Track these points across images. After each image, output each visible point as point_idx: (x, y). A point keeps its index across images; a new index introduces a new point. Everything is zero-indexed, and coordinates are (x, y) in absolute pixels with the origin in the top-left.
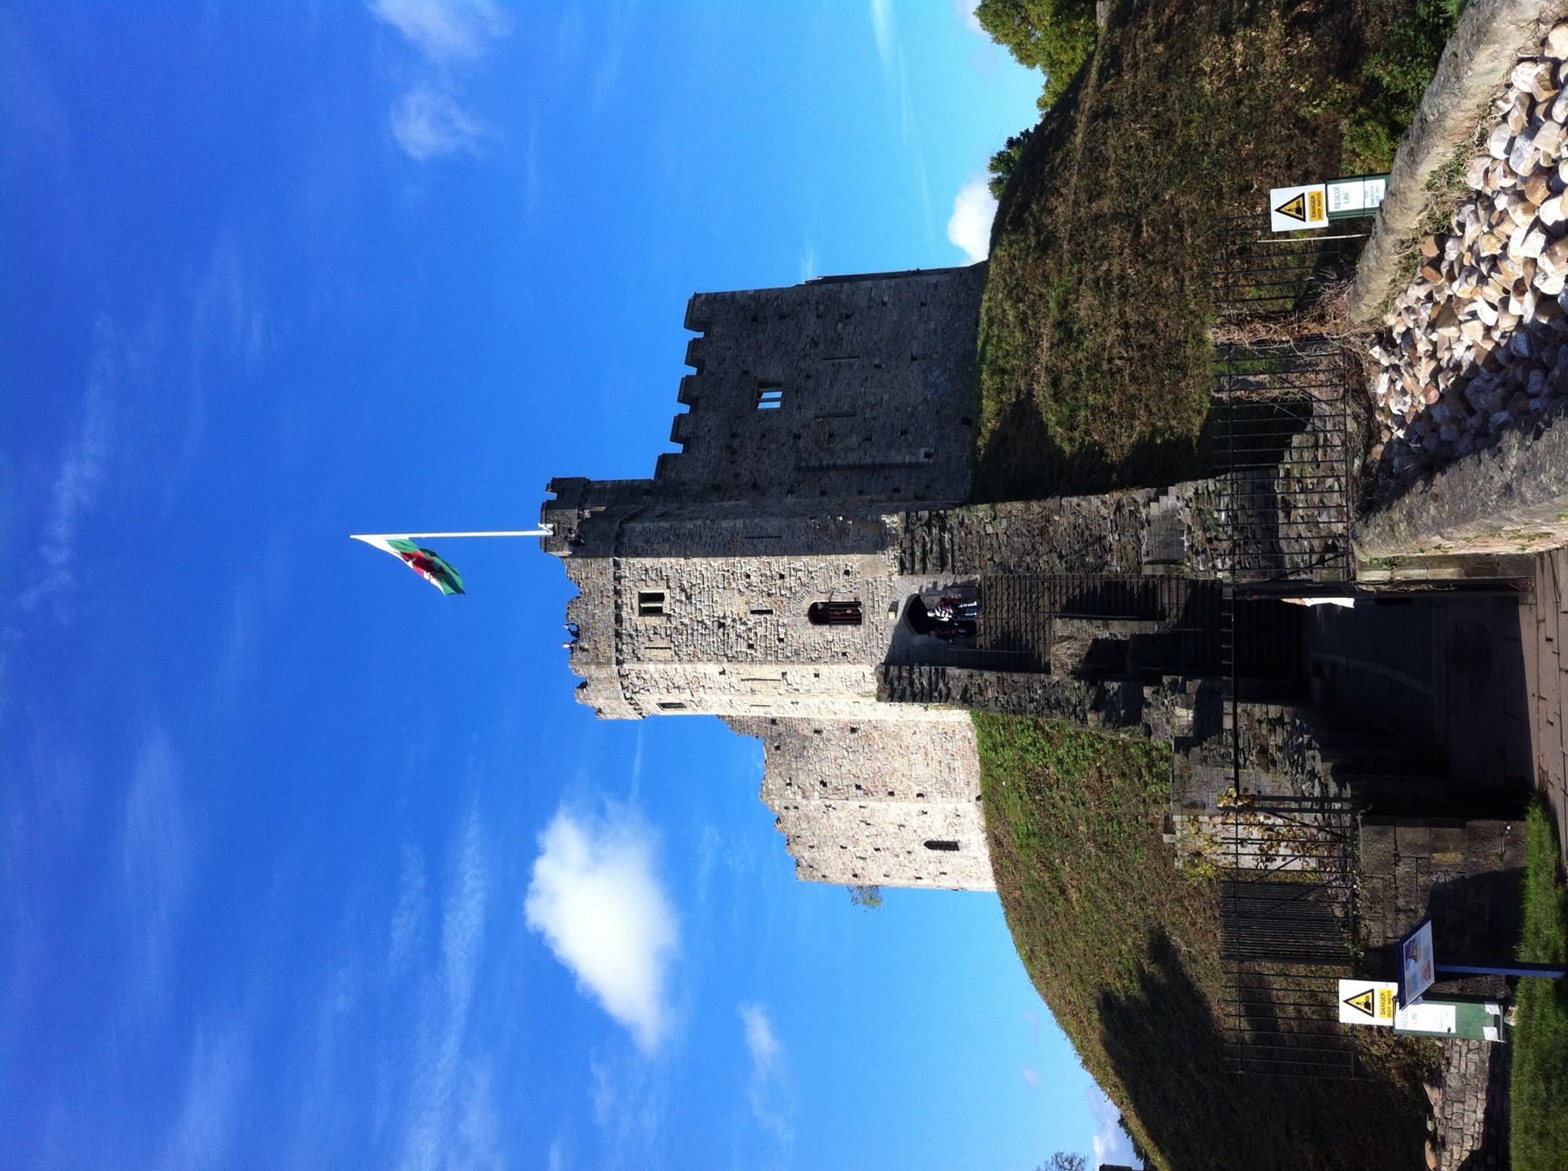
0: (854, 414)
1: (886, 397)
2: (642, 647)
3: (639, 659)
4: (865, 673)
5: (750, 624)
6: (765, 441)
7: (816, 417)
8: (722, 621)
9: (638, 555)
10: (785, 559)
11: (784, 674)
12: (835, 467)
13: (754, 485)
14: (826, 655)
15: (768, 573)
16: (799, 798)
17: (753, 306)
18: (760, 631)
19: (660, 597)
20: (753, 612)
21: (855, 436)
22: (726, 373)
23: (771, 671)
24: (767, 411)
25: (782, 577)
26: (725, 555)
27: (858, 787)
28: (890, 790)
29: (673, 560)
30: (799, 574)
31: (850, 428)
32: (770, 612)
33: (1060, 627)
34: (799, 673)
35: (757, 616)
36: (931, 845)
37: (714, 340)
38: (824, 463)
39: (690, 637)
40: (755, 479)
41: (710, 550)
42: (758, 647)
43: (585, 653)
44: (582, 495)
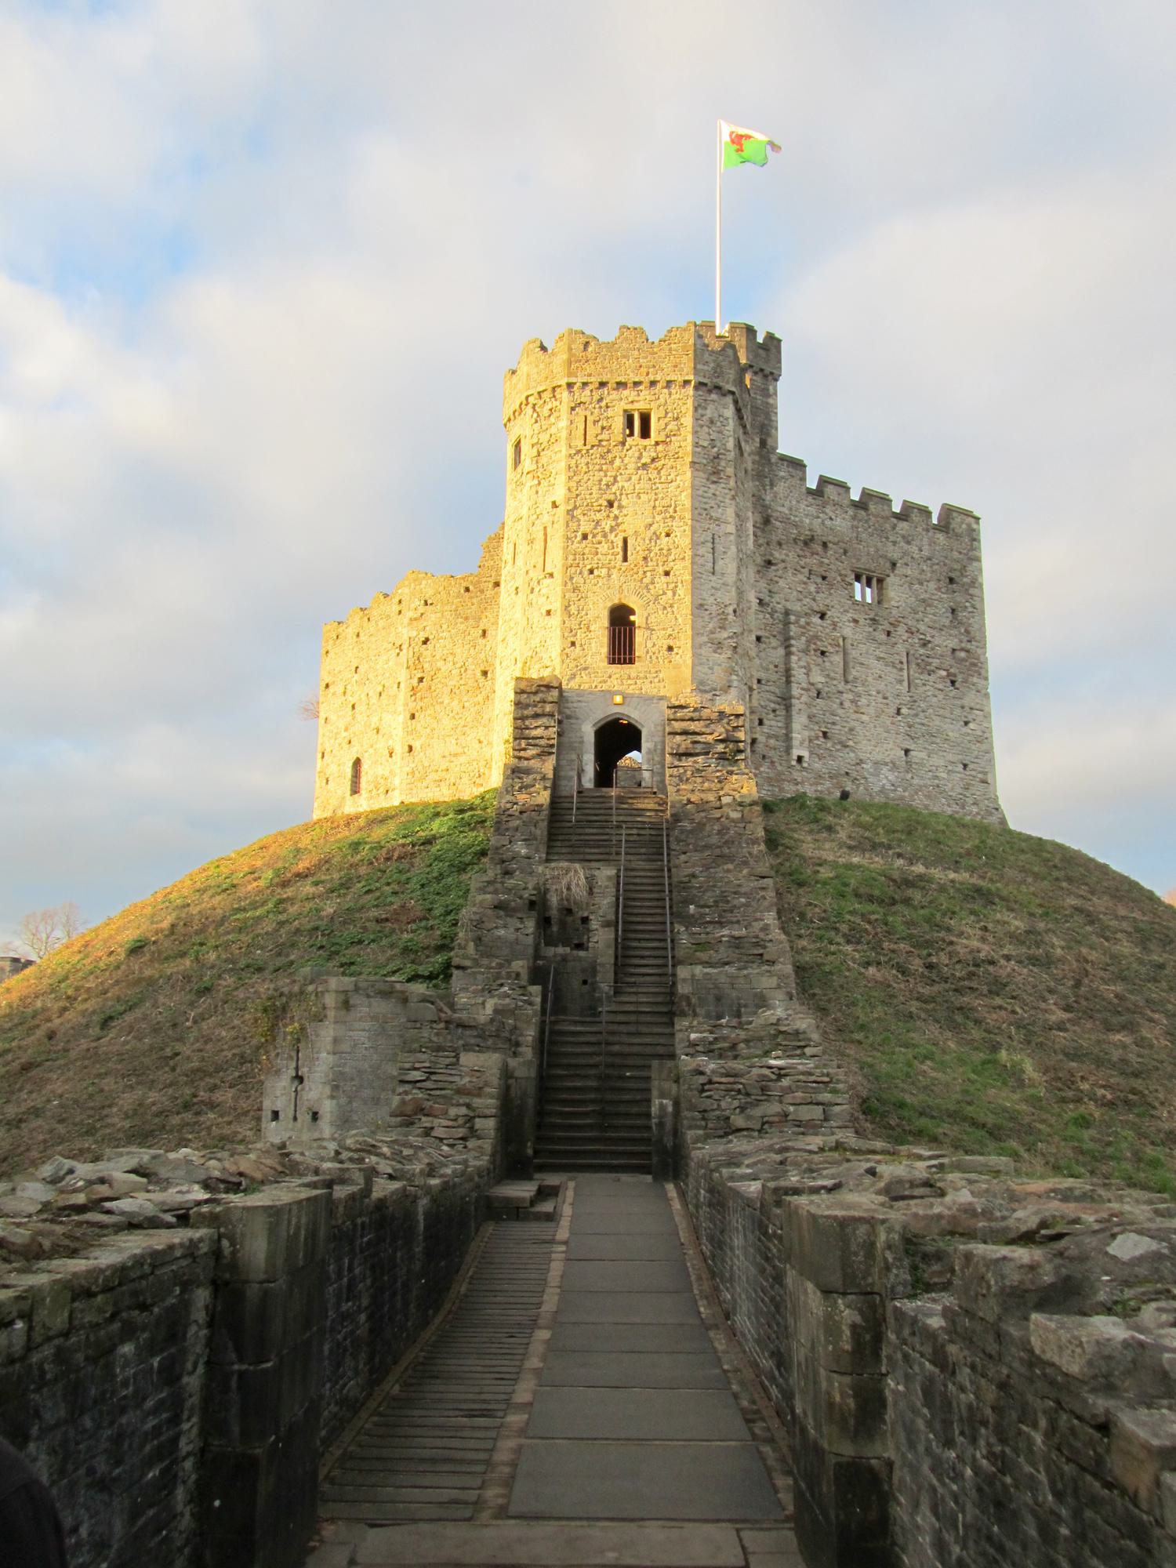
0: (847, 682)
1: (865, 718)
2: (588, 413)
3: (573, 409)
4: (550, 664)
5: (612, 537)
6: (819, 580)
7: (844, 639)
8: (616, 505)
9: (696, 409)
10: (688, 577)
11: (551, 575)
12: (788, 654)
13: (769, 563)
14: (573, 623)
15: (672, 558)
16: (411, 614)
17: (965, 580)
18: (604, 548)
19: (645, 433)
20: (625, 541)
21: (823, 680)
23: (556, 560)
25: (667, 574)
26: (694, 508)
27: (421, 680)
28: (417, 715)
29: (689, 449)
30: (670, 593)
31: (832, 674)
32: (625, 559)
33: (605, 873)
34: (552, 593)
35: (621, 544)
36: (357, 763)
37: (930, 534)
38: (793, 642)
39: (597, 467)
40: (775, 564)
41: (700, 493)
42: (583, 545)
43: (582, 347)
44: (762, 370)
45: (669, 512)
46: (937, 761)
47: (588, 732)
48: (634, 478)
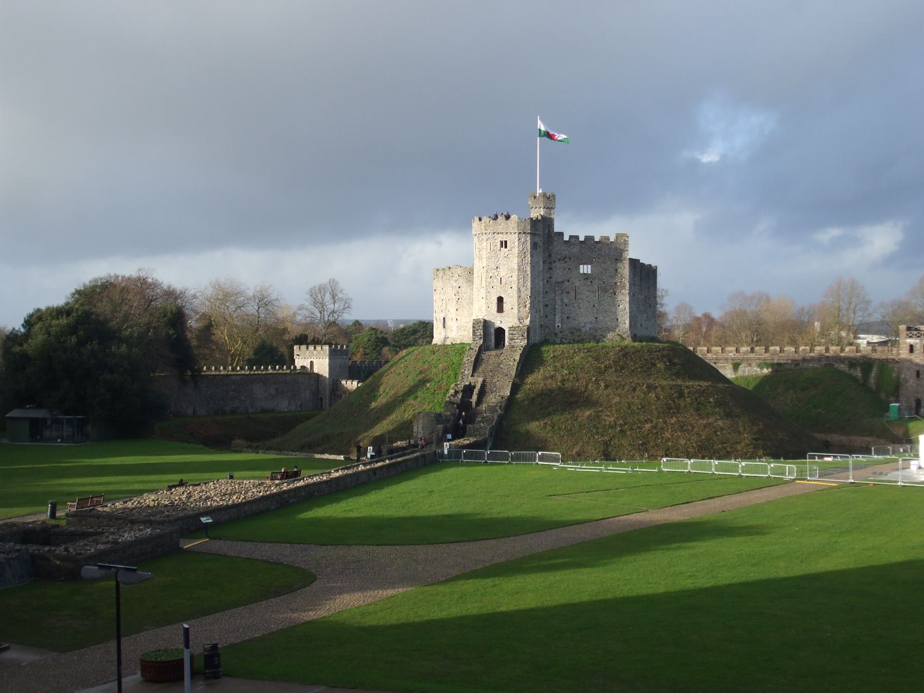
0: (576, 300)
1: (582, 310)
5: (497, 277)
12: (556, 296)
14: (488, 301)
16: (455, 279)
18: (495, 280)
19: (506, 247)
20: (501, 278)
21: (567, 301)
22: (595, 252)
23: (484, 285)
24: (579, 269)
25: (511, 288)
27: (459, 299)
32: (501, 284)
34: (483, 291)
38: (557, 293)
44: (548, 207)
45: (512, 270)
46: (607, 319)
47: (493, 331)
48: (503, 261)
